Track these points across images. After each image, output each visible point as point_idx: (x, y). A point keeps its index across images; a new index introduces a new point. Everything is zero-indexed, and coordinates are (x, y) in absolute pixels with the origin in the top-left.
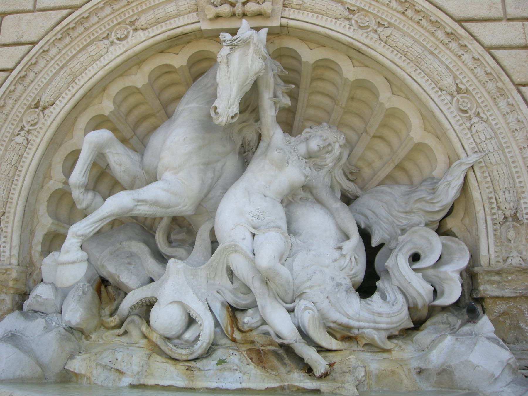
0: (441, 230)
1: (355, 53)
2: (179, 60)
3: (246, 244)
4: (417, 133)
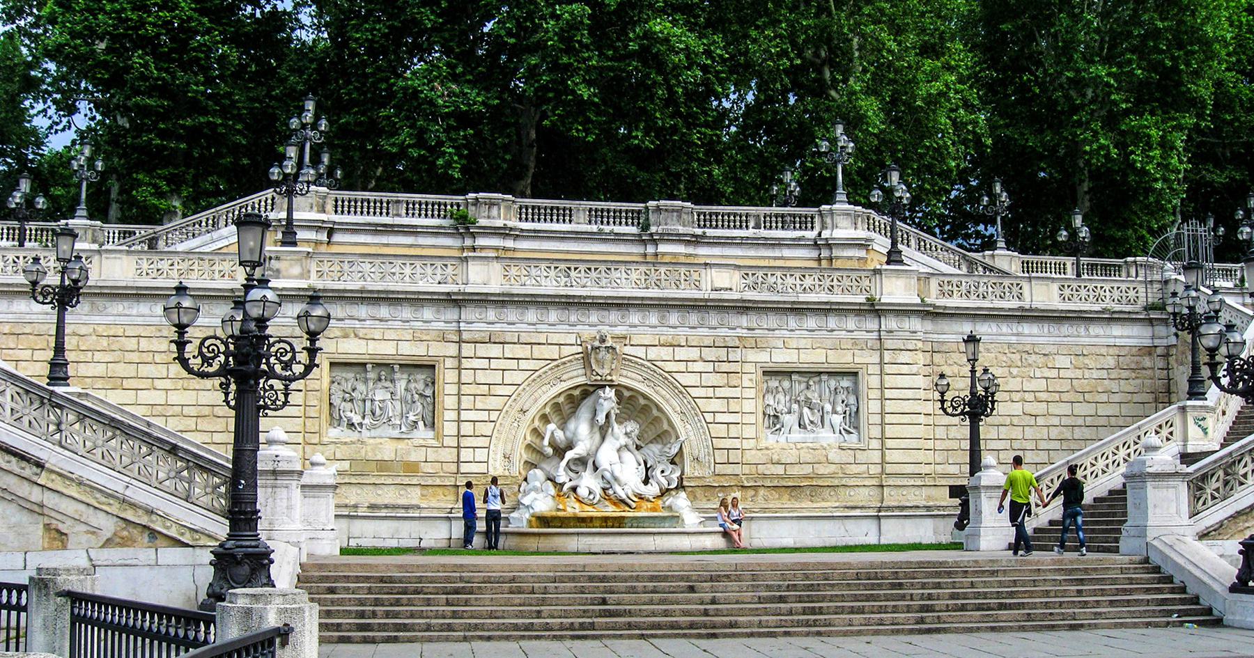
0: (673, 462)
1: (645, 397)
2: (577, 392)
3: (608, 468)
4: (666, 426)
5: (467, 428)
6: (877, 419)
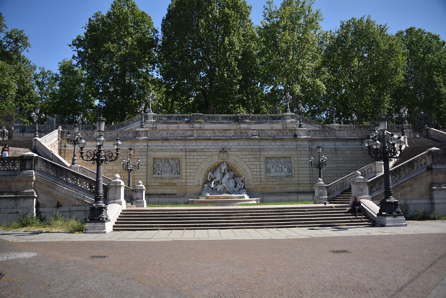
0: (242, 182)
2: (217, 164)
5: (188, 174)
6: (297, 169)
